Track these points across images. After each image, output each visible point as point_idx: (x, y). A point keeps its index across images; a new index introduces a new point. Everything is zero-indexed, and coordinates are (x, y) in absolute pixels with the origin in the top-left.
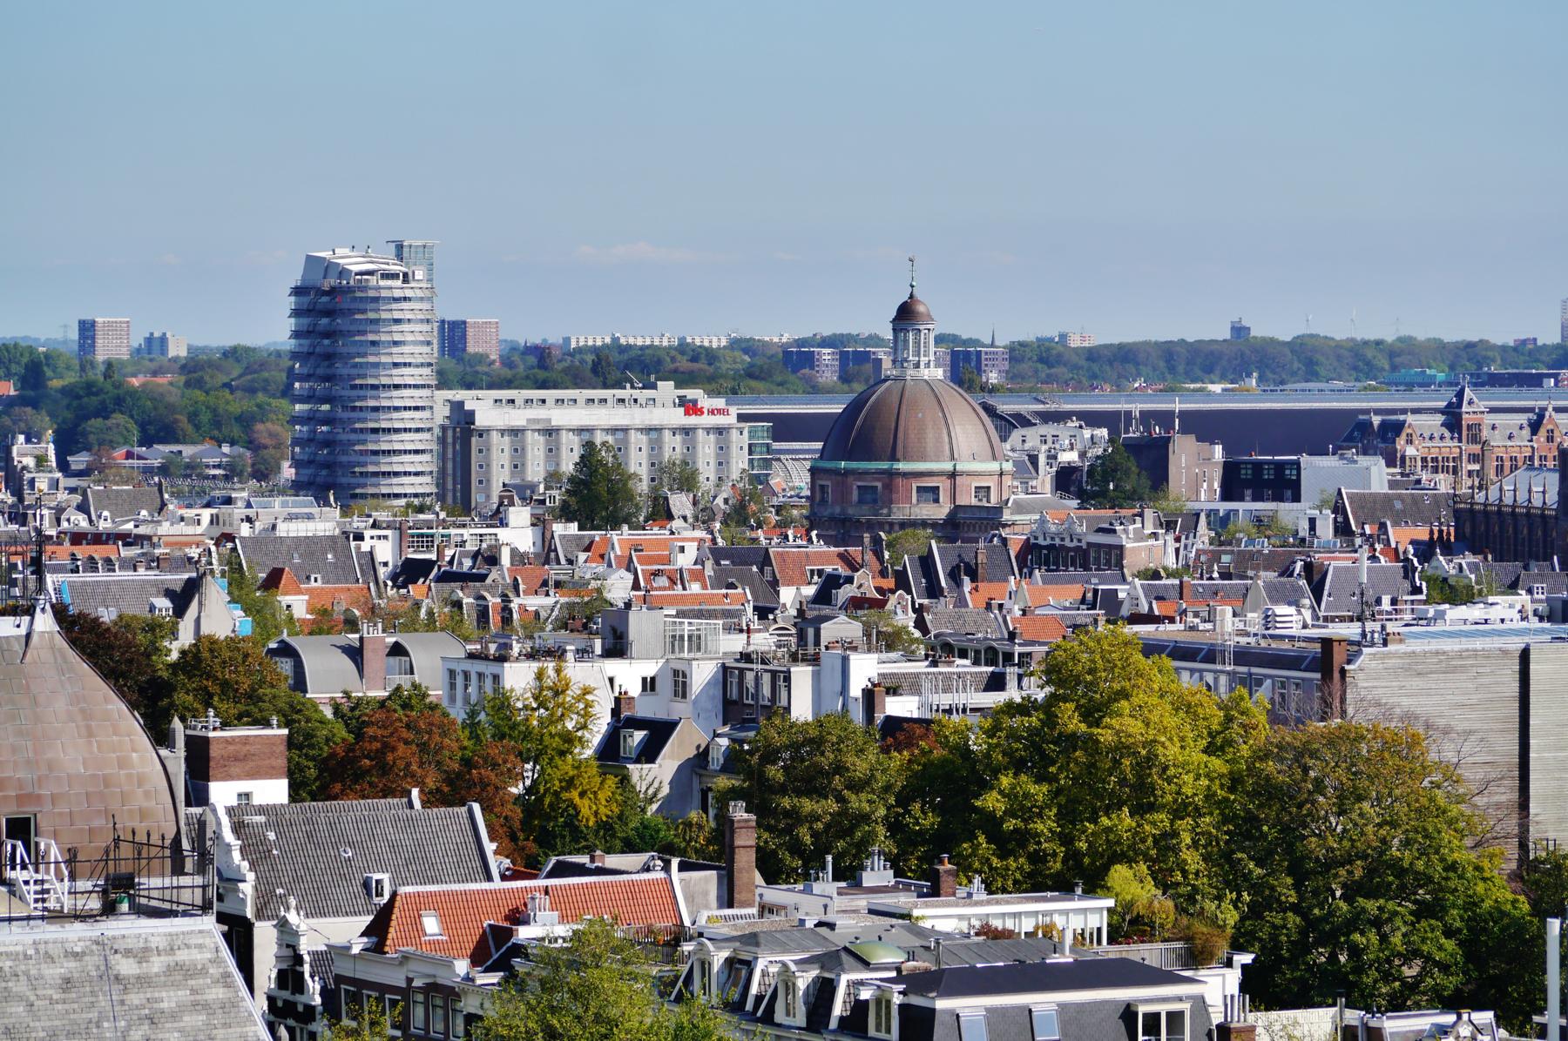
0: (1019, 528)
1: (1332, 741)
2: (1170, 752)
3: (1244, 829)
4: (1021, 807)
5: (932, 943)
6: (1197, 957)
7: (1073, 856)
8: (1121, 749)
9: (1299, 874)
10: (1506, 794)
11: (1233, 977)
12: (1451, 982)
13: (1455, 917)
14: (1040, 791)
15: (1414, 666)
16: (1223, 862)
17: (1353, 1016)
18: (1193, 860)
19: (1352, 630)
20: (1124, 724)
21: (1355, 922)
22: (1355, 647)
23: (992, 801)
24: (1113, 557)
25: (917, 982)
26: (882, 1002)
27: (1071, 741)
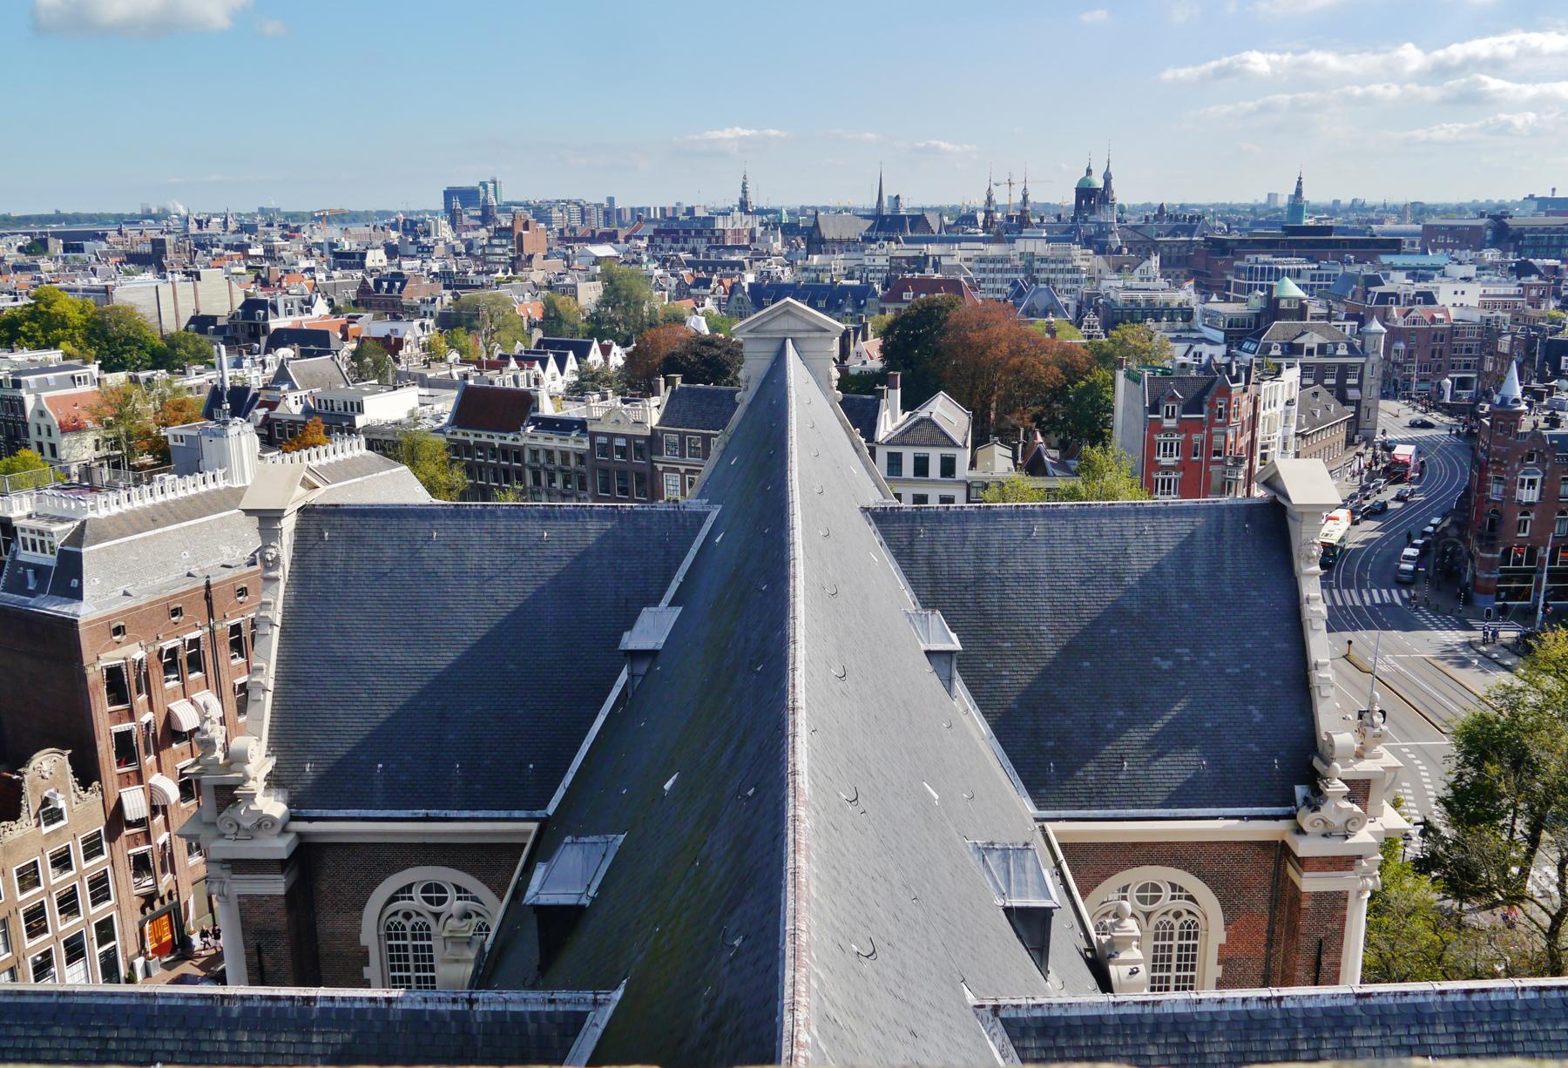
0: (10, 261)
1: (112, 309)
2: (70, 314)
3: (92, 332)
4: (31, 329)
5: (14, 364)
6: (86, 362)
7: (47, 341)
8: (56, 314)
9: (108, 342)
10: (157, 320)
11: (97, 366)
12: (149, 364)
13: (149, 349)
14: (36, 325)
15: (129, 291)
16: (86, 339)
17: (131, 373)
18: (80, 340)
19: (112, 283)
20: (56, 308)
21: (124, 352)
22: (114, 287)
23: (23, 329)
24: (37, 268)
25: (15, 373)
26: (6, 379)
27: (42, 313)
